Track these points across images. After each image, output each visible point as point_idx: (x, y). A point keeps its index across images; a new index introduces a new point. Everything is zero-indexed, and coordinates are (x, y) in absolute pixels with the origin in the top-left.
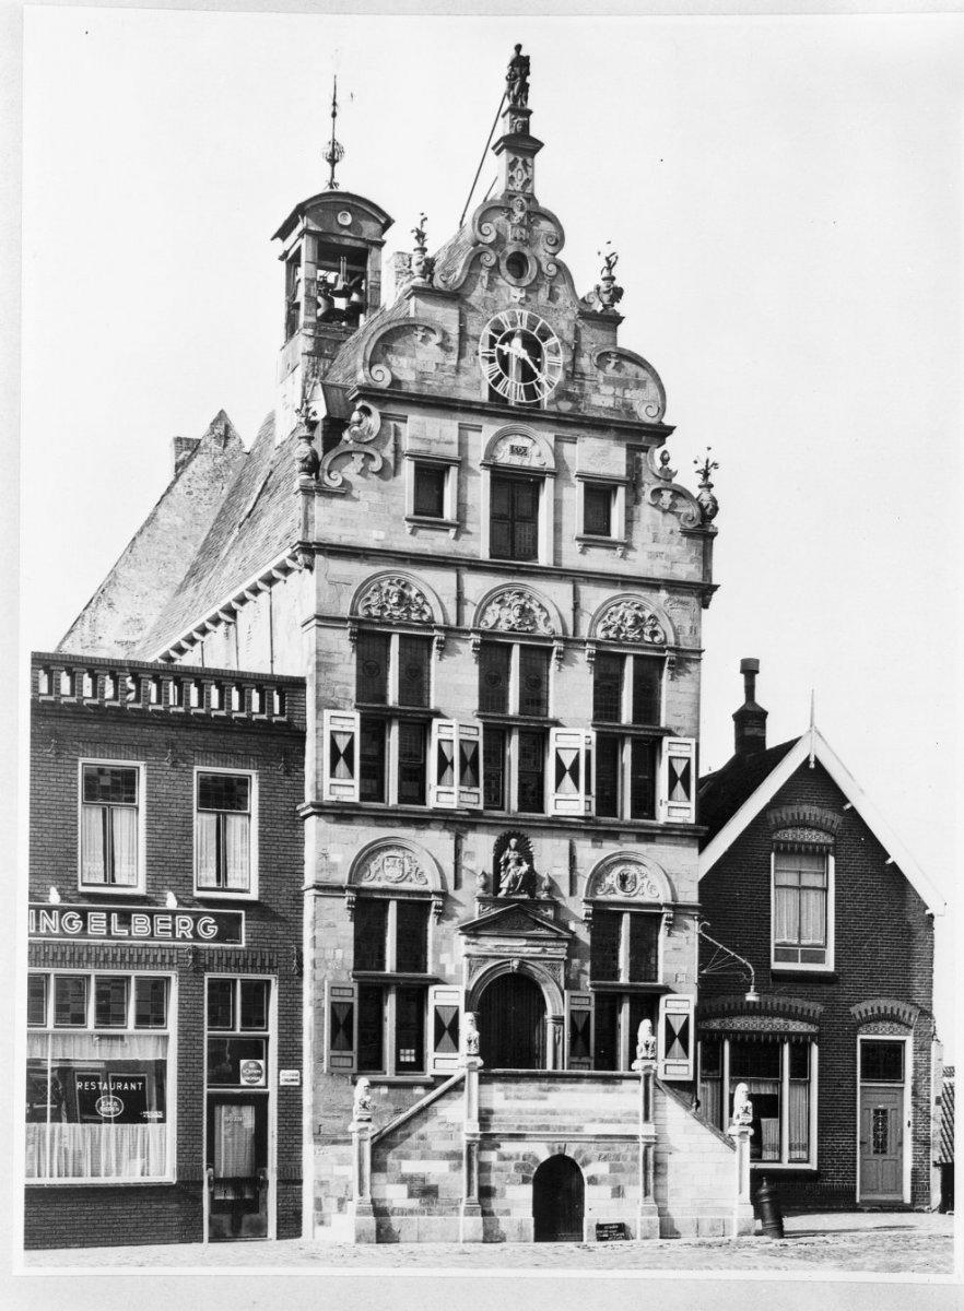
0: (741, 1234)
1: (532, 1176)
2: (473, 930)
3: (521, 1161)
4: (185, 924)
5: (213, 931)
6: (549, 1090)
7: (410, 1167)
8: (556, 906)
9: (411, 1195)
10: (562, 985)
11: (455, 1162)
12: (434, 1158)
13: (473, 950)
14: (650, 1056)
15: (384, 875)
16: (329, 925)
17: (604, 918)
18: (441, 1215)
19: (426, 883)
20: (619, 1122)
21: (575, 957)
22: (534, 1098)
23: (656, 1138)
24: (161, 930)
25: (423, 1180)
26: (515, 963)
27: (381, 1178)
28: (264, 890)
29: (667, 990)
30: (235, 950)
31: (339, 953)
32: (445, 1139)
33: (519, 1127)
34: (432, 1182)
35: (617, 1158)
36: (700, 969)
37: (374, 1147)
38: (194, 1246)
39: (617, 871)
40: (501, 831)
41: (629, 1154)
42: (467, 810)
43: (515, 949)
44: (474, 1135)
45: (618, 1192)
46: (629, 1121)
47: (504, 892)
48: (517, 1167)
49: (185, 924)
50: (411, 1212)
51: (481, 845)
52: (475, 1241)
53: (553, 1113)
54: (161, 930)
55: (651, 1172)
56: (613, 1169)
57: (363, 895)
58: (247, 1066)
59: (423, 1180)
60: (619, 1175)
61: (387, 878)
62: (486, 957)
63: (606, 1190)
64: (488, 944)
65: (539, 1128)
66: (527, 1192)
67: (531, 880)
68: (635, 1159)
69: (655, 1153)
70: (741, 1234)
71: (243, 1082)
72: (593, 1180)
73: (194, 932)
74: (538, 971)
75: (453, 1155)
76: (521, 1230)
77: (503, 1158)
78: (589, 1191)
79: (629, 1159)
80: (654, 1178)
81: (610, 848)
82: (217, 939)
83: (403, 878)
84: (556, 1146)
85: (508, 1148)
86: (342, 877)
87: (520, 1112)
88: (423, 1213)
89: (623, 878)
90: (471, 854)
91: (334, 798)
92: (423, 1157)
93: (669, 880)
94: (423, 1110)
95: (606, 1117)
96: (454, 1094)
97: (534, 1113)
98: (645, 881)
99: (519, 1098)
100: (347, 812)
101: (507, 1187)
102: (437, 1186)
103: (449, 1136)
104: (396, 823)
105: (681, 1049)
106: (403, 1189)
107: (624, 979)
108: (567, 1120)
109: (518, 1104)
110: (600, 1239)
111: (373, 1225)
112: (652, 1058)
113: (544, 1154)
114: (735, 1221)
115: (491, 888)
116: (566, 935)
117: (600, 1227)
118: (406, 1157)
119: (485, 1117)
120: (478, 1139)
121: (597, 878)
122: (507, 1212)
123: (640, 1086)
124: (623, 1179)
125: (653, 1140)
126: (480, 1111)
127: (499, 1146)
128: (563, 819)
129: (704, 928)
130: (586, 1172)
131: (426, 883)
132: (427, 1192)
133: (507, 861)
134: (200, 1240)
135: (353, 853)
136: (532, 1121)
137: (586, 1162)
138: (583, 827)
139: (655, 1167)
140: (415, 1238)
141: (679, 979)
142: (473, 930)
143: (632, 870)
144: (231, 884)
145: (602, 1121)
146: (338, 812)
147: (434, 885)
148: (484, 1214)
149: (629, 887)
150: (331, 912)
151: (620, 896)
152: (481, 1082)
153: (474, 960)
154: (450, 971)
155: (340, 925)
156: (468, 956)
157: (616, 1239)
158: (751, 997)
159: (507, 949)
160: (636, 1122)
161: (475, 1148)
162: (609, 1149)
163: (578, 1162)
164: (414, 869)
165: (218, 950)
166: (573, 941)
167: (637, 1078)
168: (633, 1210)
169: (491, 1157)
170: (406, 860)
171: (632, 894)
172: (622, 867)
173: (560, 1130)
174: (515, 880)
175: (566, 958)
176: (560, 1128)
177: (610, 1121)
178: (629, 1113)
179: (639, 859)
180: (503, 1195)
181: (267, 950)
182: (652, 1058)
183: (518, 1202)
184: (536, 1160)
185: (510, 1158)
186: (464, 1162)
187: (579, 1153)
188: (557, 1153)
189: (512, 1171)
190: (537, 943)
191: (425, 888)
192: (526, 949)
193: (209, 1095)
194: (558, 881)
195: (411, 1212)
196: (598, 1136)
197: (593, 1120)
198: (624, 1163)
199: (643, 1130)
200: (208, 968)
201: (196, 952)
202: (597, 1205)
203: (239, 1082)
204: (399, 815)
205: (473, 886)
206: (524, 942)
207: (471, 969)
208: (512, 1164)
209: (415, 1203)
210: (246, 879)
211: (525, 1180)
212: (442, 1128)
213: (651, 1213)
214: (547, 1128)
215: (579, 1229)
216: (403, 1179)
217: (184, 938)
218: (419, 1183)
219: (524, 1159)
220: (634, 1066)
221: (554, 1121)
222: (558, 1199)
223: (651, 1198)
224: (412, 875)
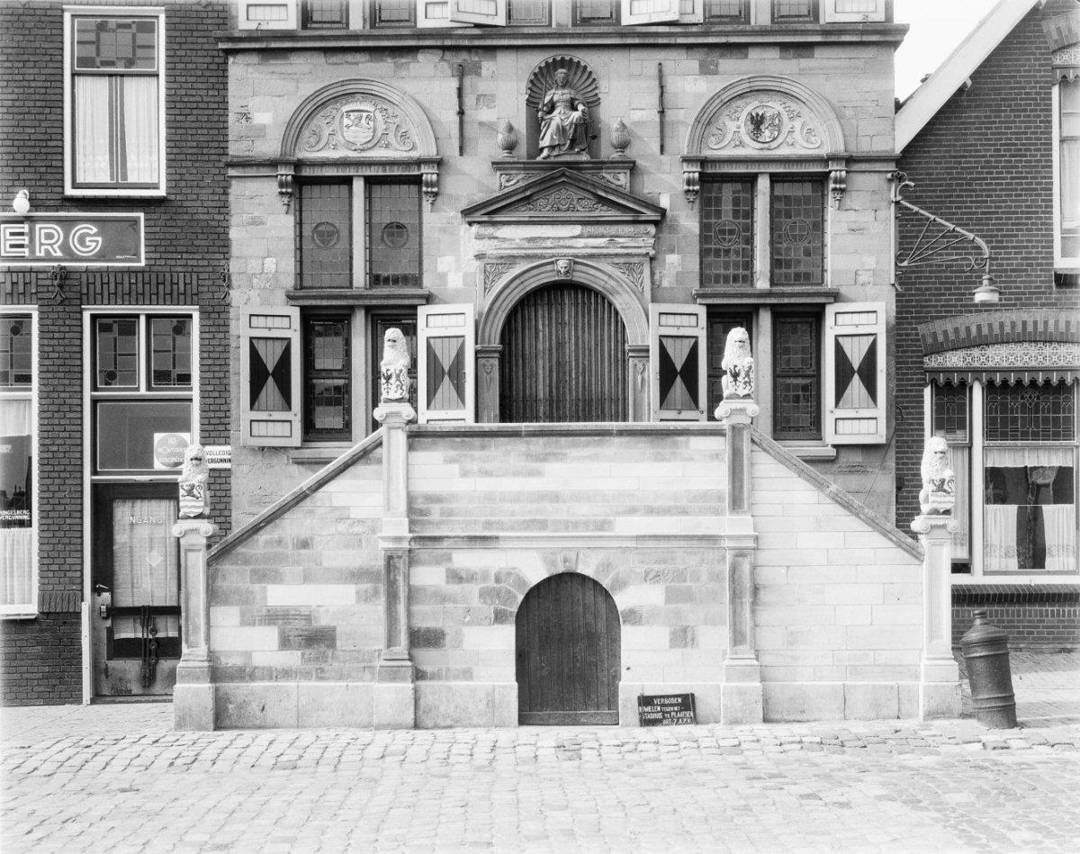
0: (932, 715)
1: (515, 609)
2: (486, 212)
3: (491, 583)
4: (49, 236)
5: (95, 243)
6: (545, 458)
7: (279, 595)
8: (632, 167)
9: (285, 643)
10: (648, 295)
11: (367, 586)
12: (327, 582)
13: (488, 247)
14: (741, 392)
15: (347, 137)
16: (255, 222)
17: (715, 183)
18: (340, 678)
19: (413, 148)
20: (685, 512)
21: (672, 251)
22: (515, 474)
23: (756, 539)
24: (12, 246)
25: (308, 618)
26: (562, 264)
27: (226, 617)
28: (175, 178)
29: (836, 297)
30: (129, 271)
31: (270, 264)
32: (346, 546)
33: (488, 525)
34: (324, 621)
35: (681, 576)
36: (899, 258)
37: (211, 562)
38: (66, 710)
39: (751, 106)
40: (536, 60)
41: (704, 569)
42: (477, 26)
43: (558, 241)
44: (399, 539)
45: (683, 637)
46: (702, 512)
47: (545, 153)
48: (483, 594)
49: (49, 236)
50: (286, 674)
51: (504, 89)
52: (397, 727)
53: (555, 498)
54: (12, 246)
55: (747, 599)
56: (671, 596)
57: (307, 172)
58: (162, 442)
59: (308, 618)
60: (684, 607)
61: (349, 145)
62: (511, 260)
63: (661, 634)
64: (514, 236)
65: (528, 525)
66: (504, 638)
67: (586, 132)
68: (716, 577)
69: (754, 567)
70: (932, 715)
71: (158, 465)
72: (634, 616)
73: (65, 247)
74: (600, 276)
75: (356, 576)
76: (491, 704)
77: (456, 577)
78: (628, 634)
79: (704, 577)
80: (753, 612)
81: (733, 70)
82: (101, 256)
83: (374, 143)
84: (560, 558)
85: (466, 560)
86: (270, 147)
87: (489, 497)
88: (306, 675)
89: (757, 122)
90: (486, 99)
91: (252, 26)
92: (307, 579)
93: (839, 117)
94: (301, 498)
95: (660, 503)
96: (360, 469)
97: (517, 498)
98: (797, 124)
99: (487, 473)
100: (274, 45)
101: (466, 630)
102: (334, 629)
103: (357, 542)
104: (359, 57)
105: (864, 391)
106: (270, 635)
107: (762, 284)
108: (583, 510)
109: (484, 485)
110: (646, 722)
111: (209, 702)
112: (747, 396)
113: (536, 573)
114: (921, 689)
115: (522, 150)
116: (650, 215)
117: (645, 701)
118: (277, 578)
119: (415, 512)
120: (406, 545)
121: (707, 120)
122: (467, 674)
123: (720, 445)
124: (691, 614)
125: (751, 544)
126: (411, 499)
127: (449, 559)
128: (644, 29)
129: (904, 191)
130: (622, 601)
131: (413, 148)
132: (315, 639)
133: (552, 107)
134: (78, 700)
135: (288, 107)
136: (513, 514)
137: (621, 584)
138: (681, 40)
139: (747, 591)
140: (293, 721)
141: (861, 279)
142: (486, 212)
143: (773, 106)
144: (132, 179)
145: (651, 511)
146: (263, 45)
147: (426, 149)
148: (419, 675)
149: (766, 134)
150: (256, 201)
151: (751, 149)
152: (411, 448)
153: (492, 266)
154: (455, 281)
155: (270, 221)
156: (479, 257)
157: (677, 721)
158: (981, 295)
159: (549, 244)
160: (717, 512)
161: (401, 565)
162: (665, 562)
163: (605, 583)
164: (393, 128)
165: (100, 271)
166: (661, 220)
167: (718, 433)
168: (706, 669)
169: (428, 576)
170: (379, 115)
171: (773, 145)
172: (756, 103)
173: (567, 528)
174: (562, 131)
175: (652, 252)
176: (568, 525)
177: (666, 511)
178: (704, 496)
179: (785, 87)
180: (458, 644)
181: (180, 269)
182: (747, 396)
183: (490, 652)
184: (520, 581)
185: (471, 578)
186: (382, 588)
187: (607, 566)
188: (560, 569)
189: (475, 602)
190: (601, 229)
191: (415, 155)
192: (581, 242)
193: (95, 486)
194: (639, 132)
195: (286, 674)
196: (638, 538)
197: (632, 511)
198: (694, 586)
199: (732, 526)
200: (84, 298)
201: (64, 276)
202: (643, 661)
203: (151, 465)
204: (362, 43)
205: (489, 148)
206: (577, 230)
207: (486, 277)
208: (473, 589)
209: (292, 658)
210: (149, 169)
211: (499, 617)
212: (341, 527)
213: (745, 675)
214: (543, 525)
215: (612, 701)
216: (272, 617)
217: (48, 258)
218: (300, 624)
219: (498, 580)
220: (718, 413)
221: (552, 512)
222: (564, 647)
223: (745, 649)
224: (391, 138)
